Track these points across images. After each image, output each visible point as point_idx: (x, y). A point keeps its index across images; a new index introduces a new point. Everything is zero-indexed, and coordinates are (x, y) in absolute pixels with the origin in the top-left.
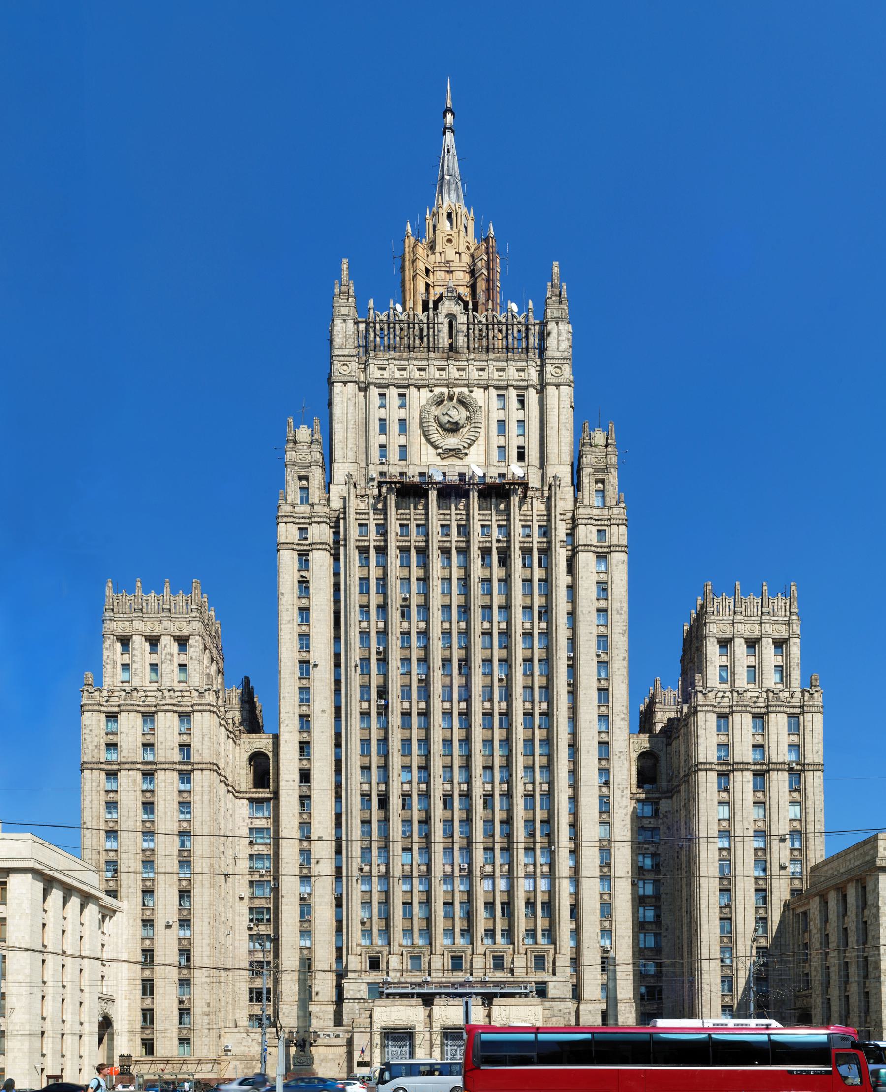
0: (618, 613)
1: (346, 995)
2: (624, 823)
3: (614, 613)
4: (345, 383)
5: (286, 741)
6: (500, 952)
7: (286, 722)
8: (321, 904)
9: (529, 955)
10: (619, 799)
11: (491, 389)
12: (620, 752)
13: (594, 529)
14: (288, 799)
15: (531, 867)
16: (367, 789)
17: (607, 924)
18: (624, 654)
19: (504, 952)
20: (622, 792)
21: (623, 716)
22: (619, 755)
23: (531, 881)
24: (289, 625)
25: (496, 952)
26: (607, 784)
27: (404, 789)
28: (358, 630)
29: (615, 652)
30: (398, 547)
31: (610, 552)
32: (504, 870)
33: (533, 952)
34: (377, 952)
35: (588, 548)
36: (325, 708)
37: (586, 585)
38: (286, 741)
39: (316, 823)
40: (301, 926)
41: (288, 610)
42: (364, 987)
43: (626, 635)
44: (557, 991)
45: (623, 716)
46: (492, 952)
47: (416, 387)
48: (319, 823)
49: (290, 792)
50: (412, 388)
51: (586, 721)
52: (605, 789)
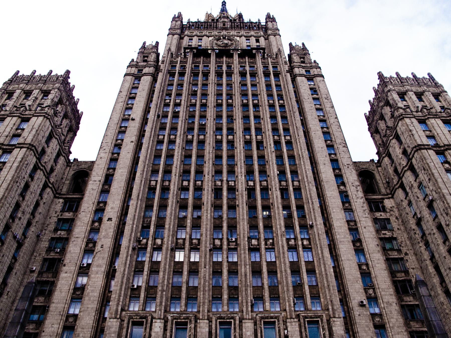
0: (326, 99)
2: (364, 208)
3: (324, 100)
4: (173, 35)
5: (101, 158)
6: (272, 318)
8: (97, 273)
9: (302, 321)
10: (355, 193)
11: (243, 37)
12: (348, 164)
13: (304, 70)
14: (92, 192)
15: (293, 241)
16: (154, 184)
17: (371, 291)
19: (276, 317)
20: (356, 188)
21: (344, 145)
22: (347, 166)
23: (295, 254)
24: (121, 104)
25: (267, 318)
26: (343, 184)
27: (184, 184)
28: (163, 103)
29: (329, 115)
30: (192, 73)
31: (315, 77)
32: (268, 243)
33: (305, 317)
34: (141, 318)
35: (301, 75)
37: (304, 88)
40: (73, 293)
41: (122, 97)
45: (344, 145)
46: (262, 318)
47: (207, 36)
48: (112, 208)
49: (94, 188)
50: (205, 37)
52: (342, 187)
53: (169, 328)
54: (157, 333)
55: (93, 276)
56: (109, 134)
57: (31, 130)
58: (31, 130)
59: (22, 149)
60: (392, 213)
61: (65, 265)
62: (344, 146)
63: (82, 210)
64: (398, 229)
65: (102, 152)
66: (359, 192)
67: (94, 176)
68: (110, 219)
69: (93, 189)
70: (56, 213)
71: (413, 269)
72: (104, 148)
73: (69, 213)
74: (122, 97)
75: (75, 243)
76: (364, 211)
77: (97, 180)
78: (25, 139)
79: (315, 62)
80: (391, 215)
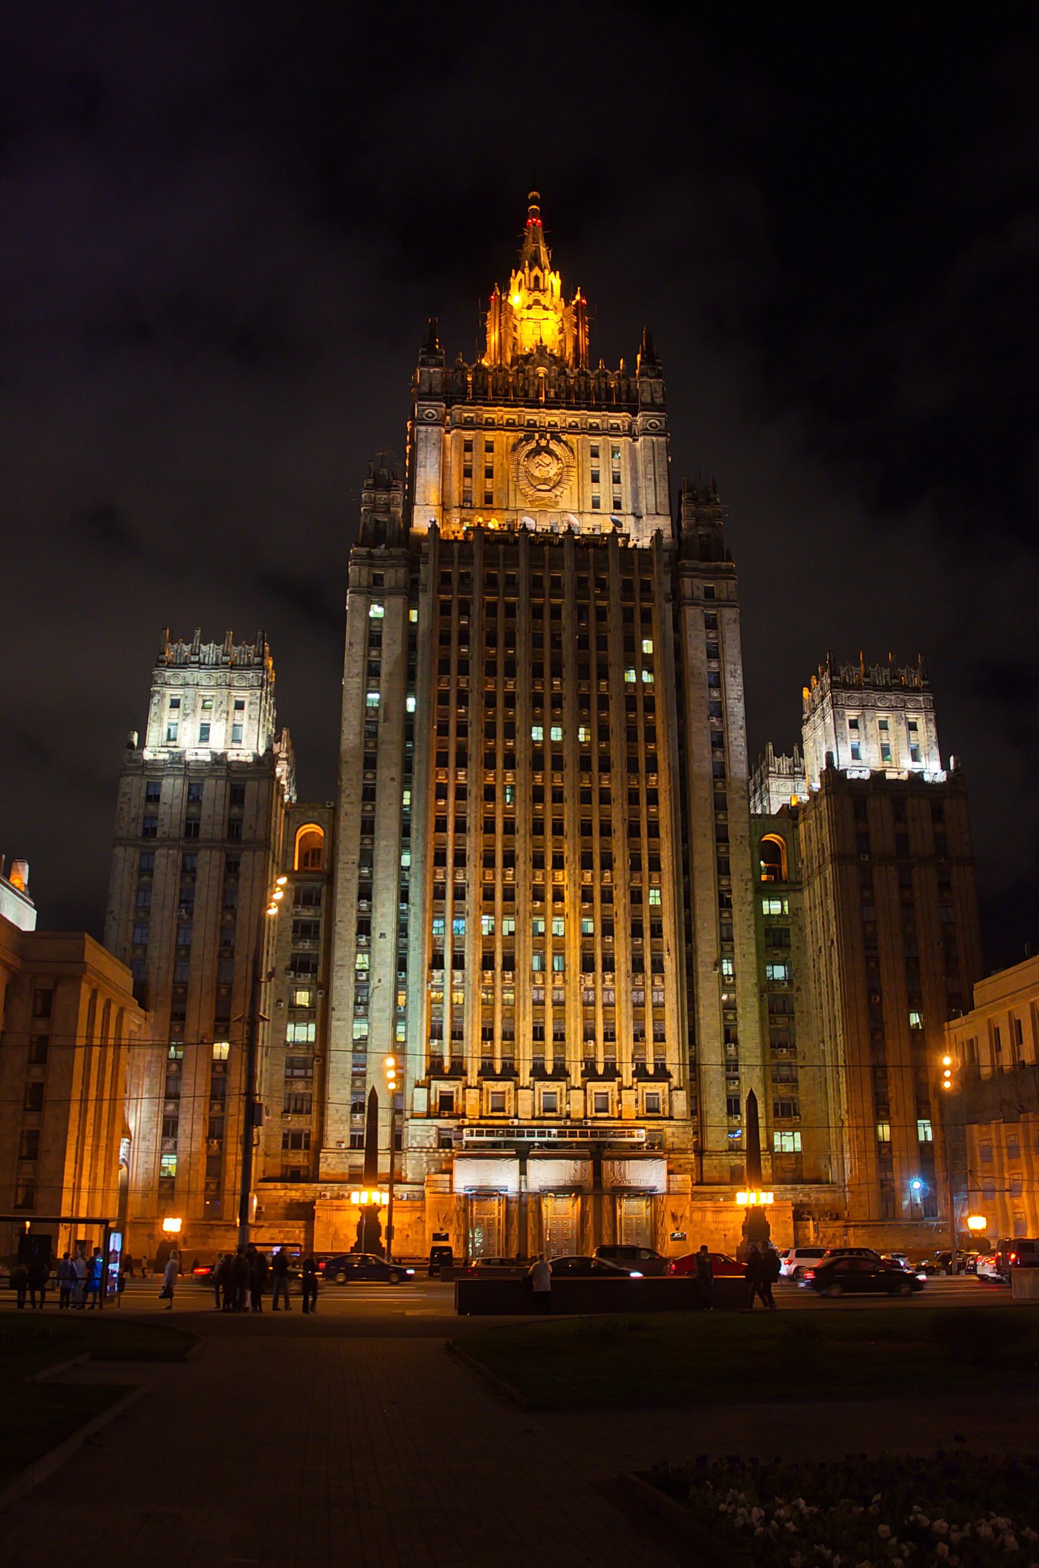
0: (732, 676)
1: (409, 1142)
3: (728, 675)
5: (346, 814)
7: (348, 792)
8: (380, 1021)
10: (743, 894)
12: (742, 837)
14: (345, 884)
18: (742, 722)
22: (740, 840)
36: (394, 775)
38: (346, 814)
39: (378, 915)
41: (356, 662)
42: (433, 1132)
43: (742, 701)
44: (676, 1140)
51: (701, 798)
53: (484, 1098)
54: (472, 1106)
55: (375, 1025)
56: (351, 759)
57: (258, 812)
58: (258, 812)
59: (257, 853)
60: (795, 918)
61: (333, 1009)
62: (743, 797)
63: (338, 919)
64: (798, 948)
65: (346, 800)
66: (748, 893)
67: (343, 854)
68: (382, 935)
69: (347, 880)
70: (288, 911)
71: (802, 1012)
72: (348, 792)
73: (308, 910)
74: (356, 662)
75: (339, 974)
76: (749, 926)
77: (350, 862)
78: (255, 832)
79: (728, 551)
80: (793, 923)
